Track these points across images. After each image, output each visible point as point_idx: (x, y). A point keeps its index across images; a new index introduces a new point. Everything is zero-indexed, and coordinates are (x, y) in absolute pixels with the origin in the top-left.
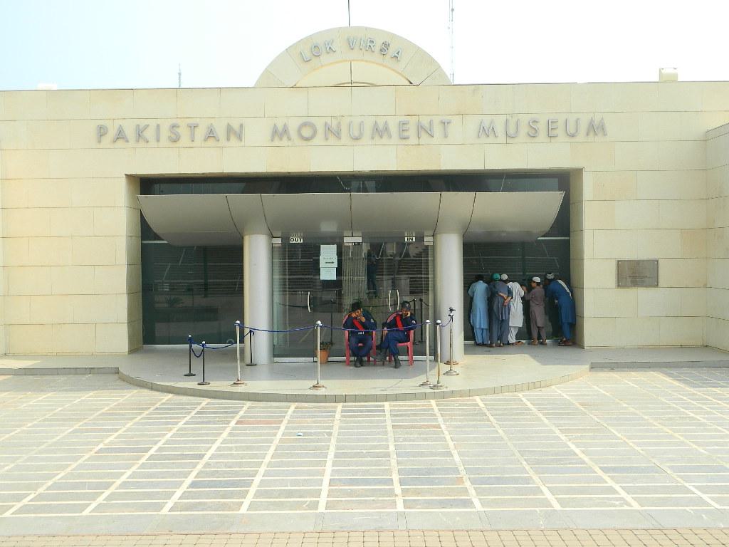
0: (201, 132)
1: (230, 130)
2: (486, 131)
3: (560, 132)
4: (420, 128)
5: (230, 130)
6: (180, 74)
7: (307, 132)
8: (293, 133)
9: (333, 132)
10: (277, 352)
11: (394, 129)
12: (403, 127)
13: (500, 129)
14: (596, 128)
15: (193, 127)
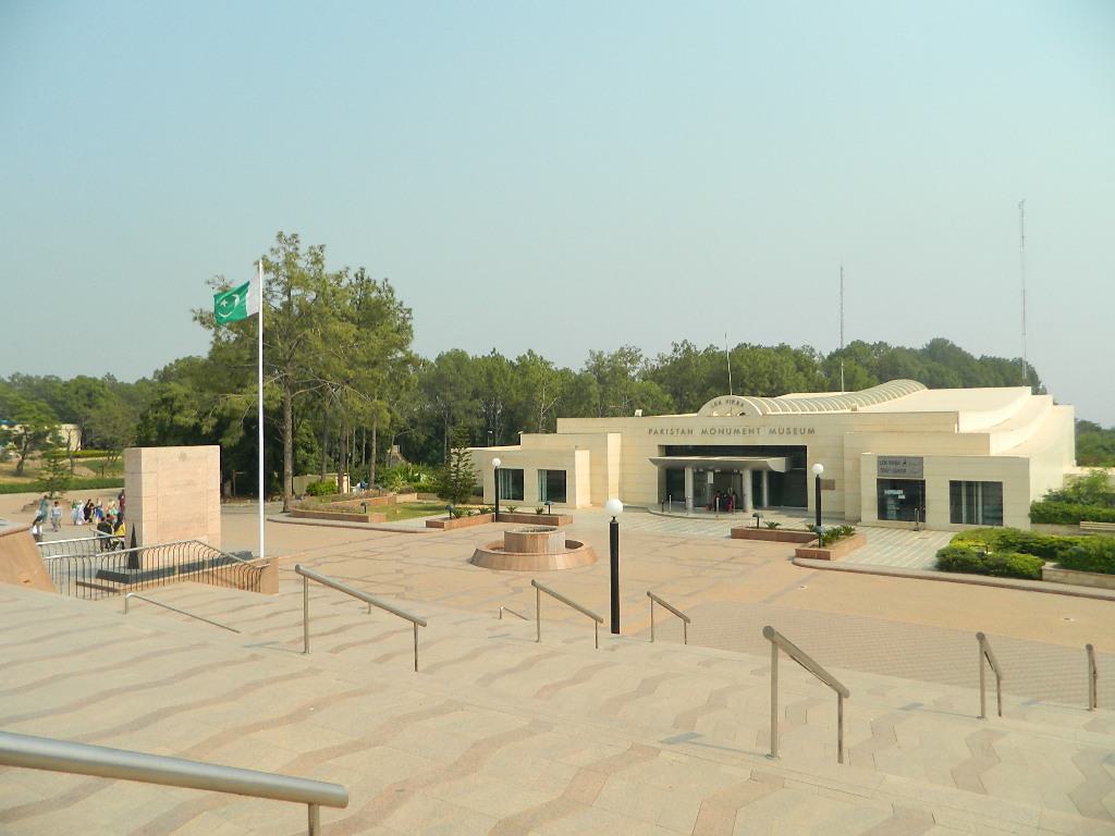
0: (680, 431)
2: (772, 432)
6: (842, 269)
10: (695, 506)
12: (744, 431)
13: (777, 431)
14: (811, 431)
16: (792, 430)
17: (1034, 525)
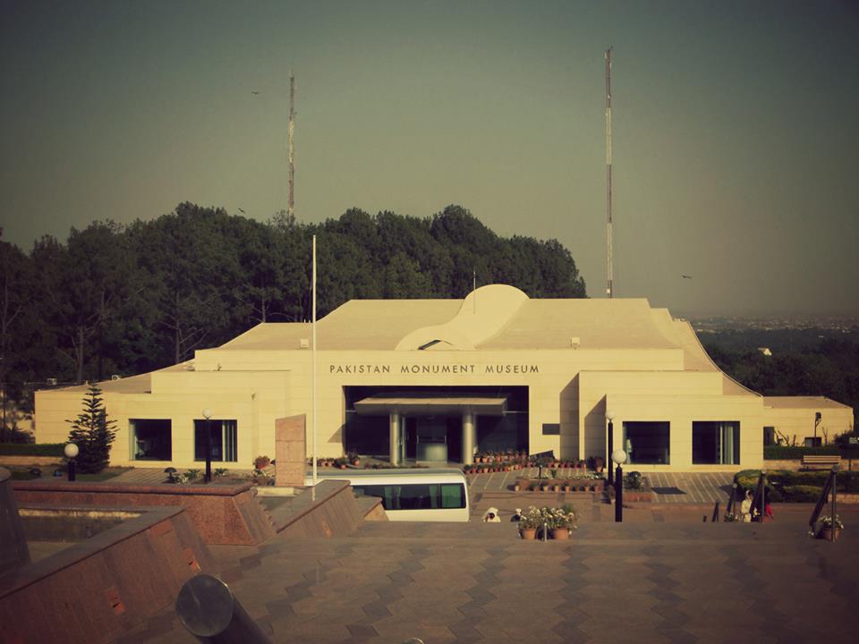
0: (372, 369)
1: (384, 367)
2: (489, 369)
3: (520, 370)
5: (384, 367)
7: (415, 369)
8: (410, 369)
14: (534, 369)
15: (369, 367)
17: (768, 461)
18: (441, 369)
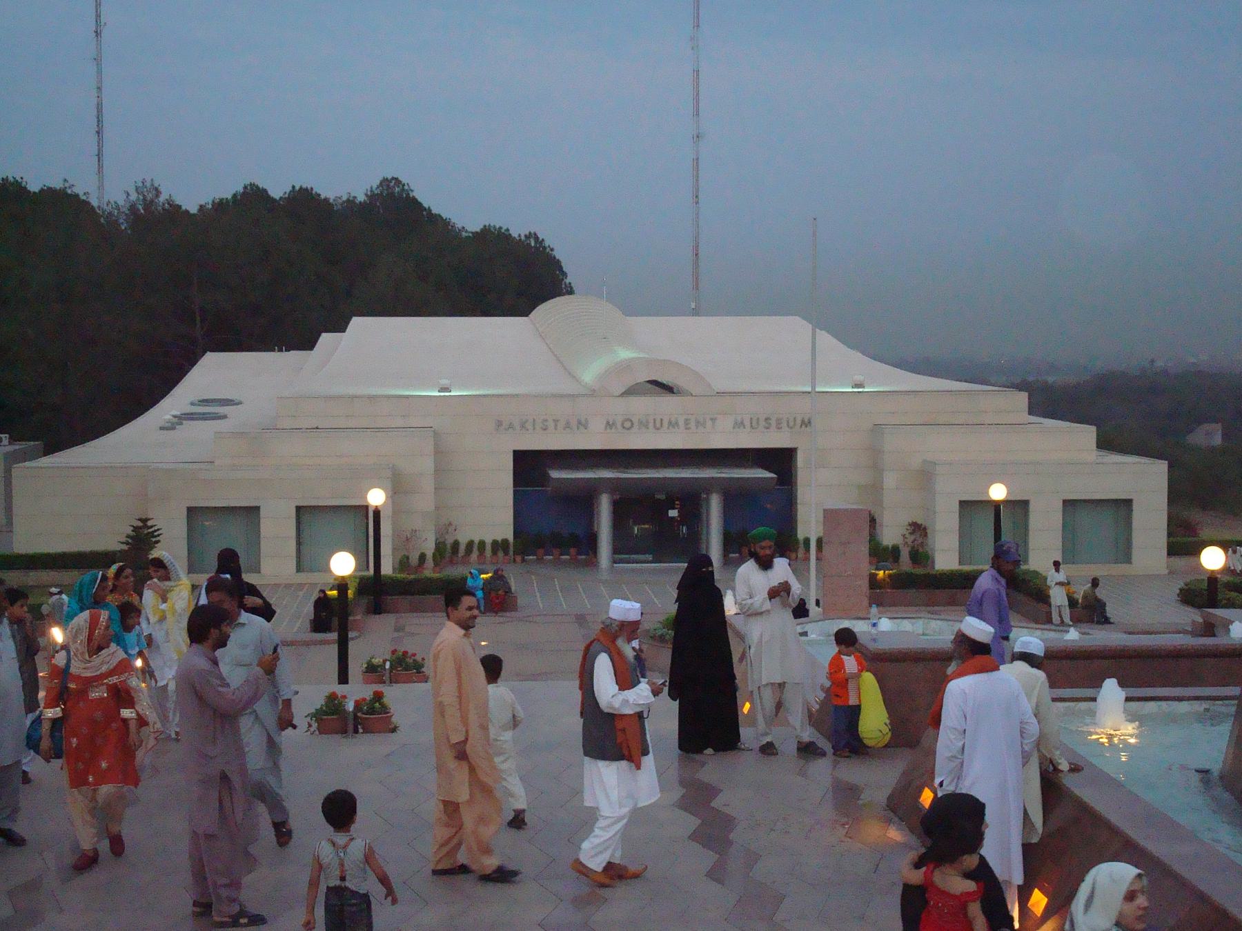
1: (579, 423)
2: (739, 424)
4: (698, 423)
5: (579, 423)
7: (628, 424)
9: (644, 424)
11: (681, 423)
12: (687, 422)
13: (747, 423)
14: (806, 423)
16: (773, 422)
18: (666, 424)
